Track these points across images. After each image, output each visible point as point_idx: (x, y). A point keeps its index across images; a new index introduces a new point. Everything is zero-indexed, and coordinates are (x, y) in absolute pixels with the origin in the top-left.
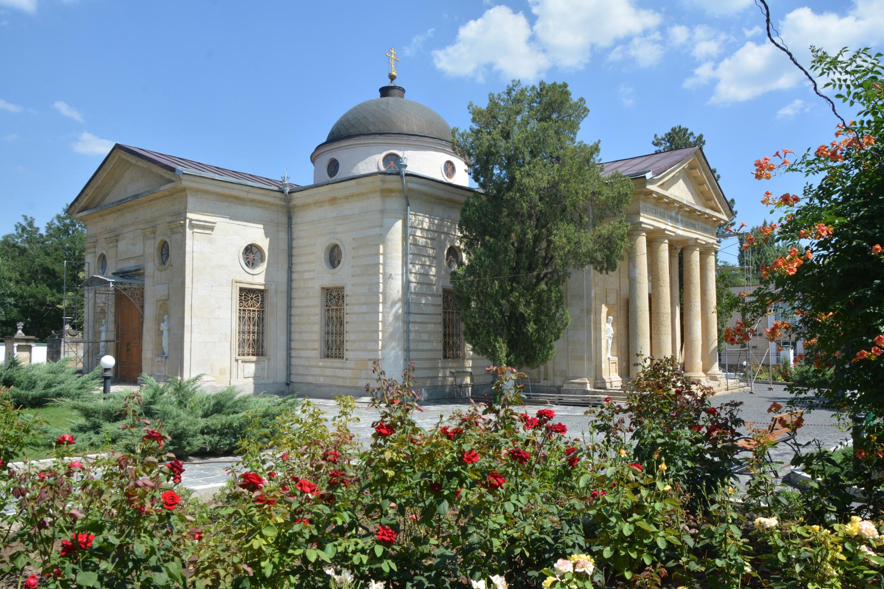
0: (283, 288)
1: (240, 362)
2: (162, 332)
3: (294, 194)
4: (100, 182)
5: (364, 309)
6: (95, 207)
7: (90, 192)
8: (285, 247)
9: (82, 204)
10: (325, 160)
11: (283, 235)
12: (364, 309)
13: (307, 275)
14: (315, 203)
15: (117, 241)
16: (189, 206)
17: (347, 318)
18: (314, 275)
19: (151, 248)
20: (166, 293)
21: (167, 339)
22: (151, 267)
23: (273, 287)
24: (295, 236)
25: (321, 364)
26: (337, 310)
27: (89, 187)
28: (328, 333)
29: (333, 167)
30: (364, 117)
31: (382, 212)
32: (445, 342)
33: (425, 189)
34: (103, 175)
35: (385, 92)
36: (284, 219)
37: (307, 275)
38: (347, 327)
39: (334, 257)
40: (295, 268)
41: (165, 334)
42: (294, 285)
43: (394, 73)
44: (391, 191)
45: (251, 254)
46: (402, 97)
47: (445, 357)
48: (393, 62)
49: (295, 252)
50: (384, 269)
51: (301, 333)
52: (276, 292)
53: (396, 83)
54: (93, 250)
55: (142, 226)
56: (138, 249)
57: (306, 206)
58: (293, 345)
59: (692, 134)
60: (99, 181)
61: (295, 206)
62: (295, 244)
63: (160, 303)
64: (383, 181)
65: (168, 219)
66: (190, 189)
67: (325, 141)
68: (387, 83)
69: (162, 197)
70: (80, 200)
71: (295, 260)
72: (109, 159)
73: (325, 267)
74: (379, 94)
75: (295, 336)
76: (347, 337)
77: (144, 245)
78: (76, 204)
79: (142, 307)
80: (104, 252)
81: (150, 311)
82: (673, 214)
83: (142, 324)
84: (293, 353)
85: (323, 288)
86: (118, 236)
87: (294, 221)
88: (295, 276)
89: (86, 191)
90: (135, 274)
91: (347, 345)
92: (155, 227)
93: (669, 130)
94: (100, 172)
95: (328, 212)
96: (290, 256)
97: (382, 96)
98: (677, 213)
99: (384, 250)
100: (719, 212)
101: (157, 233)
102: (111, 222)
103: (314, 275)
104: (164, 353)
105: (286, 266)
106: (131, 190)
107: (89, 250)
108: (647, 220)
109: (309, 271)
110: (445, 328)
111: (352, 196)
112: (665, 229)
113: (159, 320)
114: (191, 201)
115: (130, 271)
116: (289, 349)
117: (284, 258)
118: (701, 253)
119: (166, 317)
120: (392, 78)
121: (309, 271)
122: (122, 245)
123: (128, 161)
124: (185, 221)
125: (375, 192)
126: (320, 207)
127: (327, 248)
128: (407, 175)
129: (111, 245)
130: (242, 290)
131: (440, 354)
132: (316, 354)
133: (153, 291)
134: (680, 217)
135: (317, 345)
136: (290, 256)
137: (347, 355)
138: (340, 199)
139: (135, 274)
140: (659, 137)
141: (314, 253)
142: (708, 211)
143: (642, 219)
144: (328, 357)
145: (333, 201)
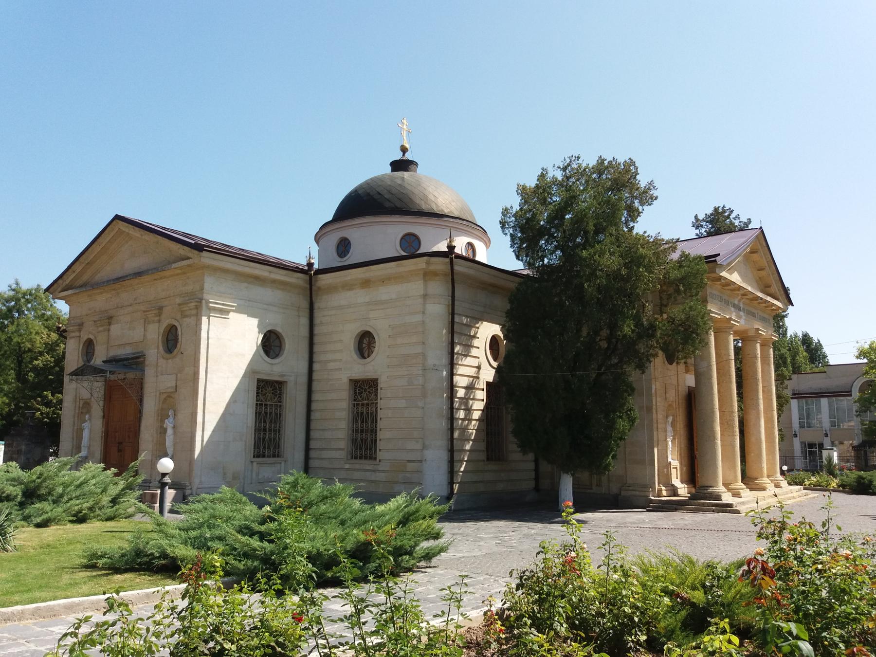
0: (304, 379)
1: (255, 464)
2: (165, 430)
5: (402, 403)
6: (81, 286)
7: (78, 268)
9: (67, 282)
10: (333, 239)
11: (305, 321)
13: (331, 366)
15: (110, 324)
16: (207, 286)
17: (380, 414)
18: (341, 365)
19: (155, 333)
21: (172, 437)
22: (154, 353)
23: (292, 378)
24: (317, 321)
25: (347, 466)
26: (368, 404)
27: (77, 263)
28: (357, 431)
29: (344, 247)
30: (379, 193)
31: (425, 296)
32: (488, 442)
33: (471, 272)
34: (97, 248)
36: (305, 304)
37: (331, 366)
38: (381, 424)
39: (365, 343)
40: (316, 358)
41: (170, 431)
42: (315, 376)
43: (407, 146)
44: (435, 274)
45: (271, 343)
46: (415, 171)
47: (488, 459)
48: (404, 134)
49: (316, 339)
51: (323, 430)
52: (296, 383)
53: (409, 156)
54: (77, 334)
55: (142, 308)
56: (137, 334)
57: (332, 289)
58: (313, 444)
59: (738, 217)
60: (90, 256)
61: (319, 288)
62: (317, 330)
64: (428, 263)
65: (178, 300)
66: (208, 267)
67: (330, 219)
68: (398, 156)
69: (172, 276)
70: (64, 277)
71: (316, 348)
72: (107, 231)
73: (355, 357)
76: (381, 435)
78: (60, 281)
79: (141, 401)
80: (91, 337)
81: (150, 406)
82: (736, 302)
83: (139, 420)
84: (312, 454)
85: (351, 380)
86: (111, 318)
87: (316, 306)
88: (316, 366)
90: (134, 362)
91: (380, 445)
92: (161, 308)
93: (710, 211)
94: (94, 246)
95: (360, 296)
96: (311, 344)
97: (393, 170)
98: (739, 301)
100: (777, 299)
101: (163, 316)
102: (101, 301)
103: (341, 365)
105: (306, 356)
106: (132, 265)
107: (72, 334)
108: (715, 310)
109: (335, 361)
110: (487, 425)
112: (730, 319)
113: (162, 416)
114: (209, 282)
115: (127, 359)
116: (307, 449)
118: (761, 346)
119: (171, 413)
120: (404, 150)
121: (335, 361)
122: (115, 329)
123: (128, 234)
127: (358, 335)
129: (101, 329)
130: (259, 380)
131: (483, 456)
132: (342, 454)
133: (156, 381)
134: (741, 305)
135: (342, 444)
136: (311, 344)
137: (380, 455)
139: (134, 362)
140: (701, 217)
141: (341, 341)
142: (769, 299)
143: (710, 307)
144: (356, 458)
145: (366, 283)
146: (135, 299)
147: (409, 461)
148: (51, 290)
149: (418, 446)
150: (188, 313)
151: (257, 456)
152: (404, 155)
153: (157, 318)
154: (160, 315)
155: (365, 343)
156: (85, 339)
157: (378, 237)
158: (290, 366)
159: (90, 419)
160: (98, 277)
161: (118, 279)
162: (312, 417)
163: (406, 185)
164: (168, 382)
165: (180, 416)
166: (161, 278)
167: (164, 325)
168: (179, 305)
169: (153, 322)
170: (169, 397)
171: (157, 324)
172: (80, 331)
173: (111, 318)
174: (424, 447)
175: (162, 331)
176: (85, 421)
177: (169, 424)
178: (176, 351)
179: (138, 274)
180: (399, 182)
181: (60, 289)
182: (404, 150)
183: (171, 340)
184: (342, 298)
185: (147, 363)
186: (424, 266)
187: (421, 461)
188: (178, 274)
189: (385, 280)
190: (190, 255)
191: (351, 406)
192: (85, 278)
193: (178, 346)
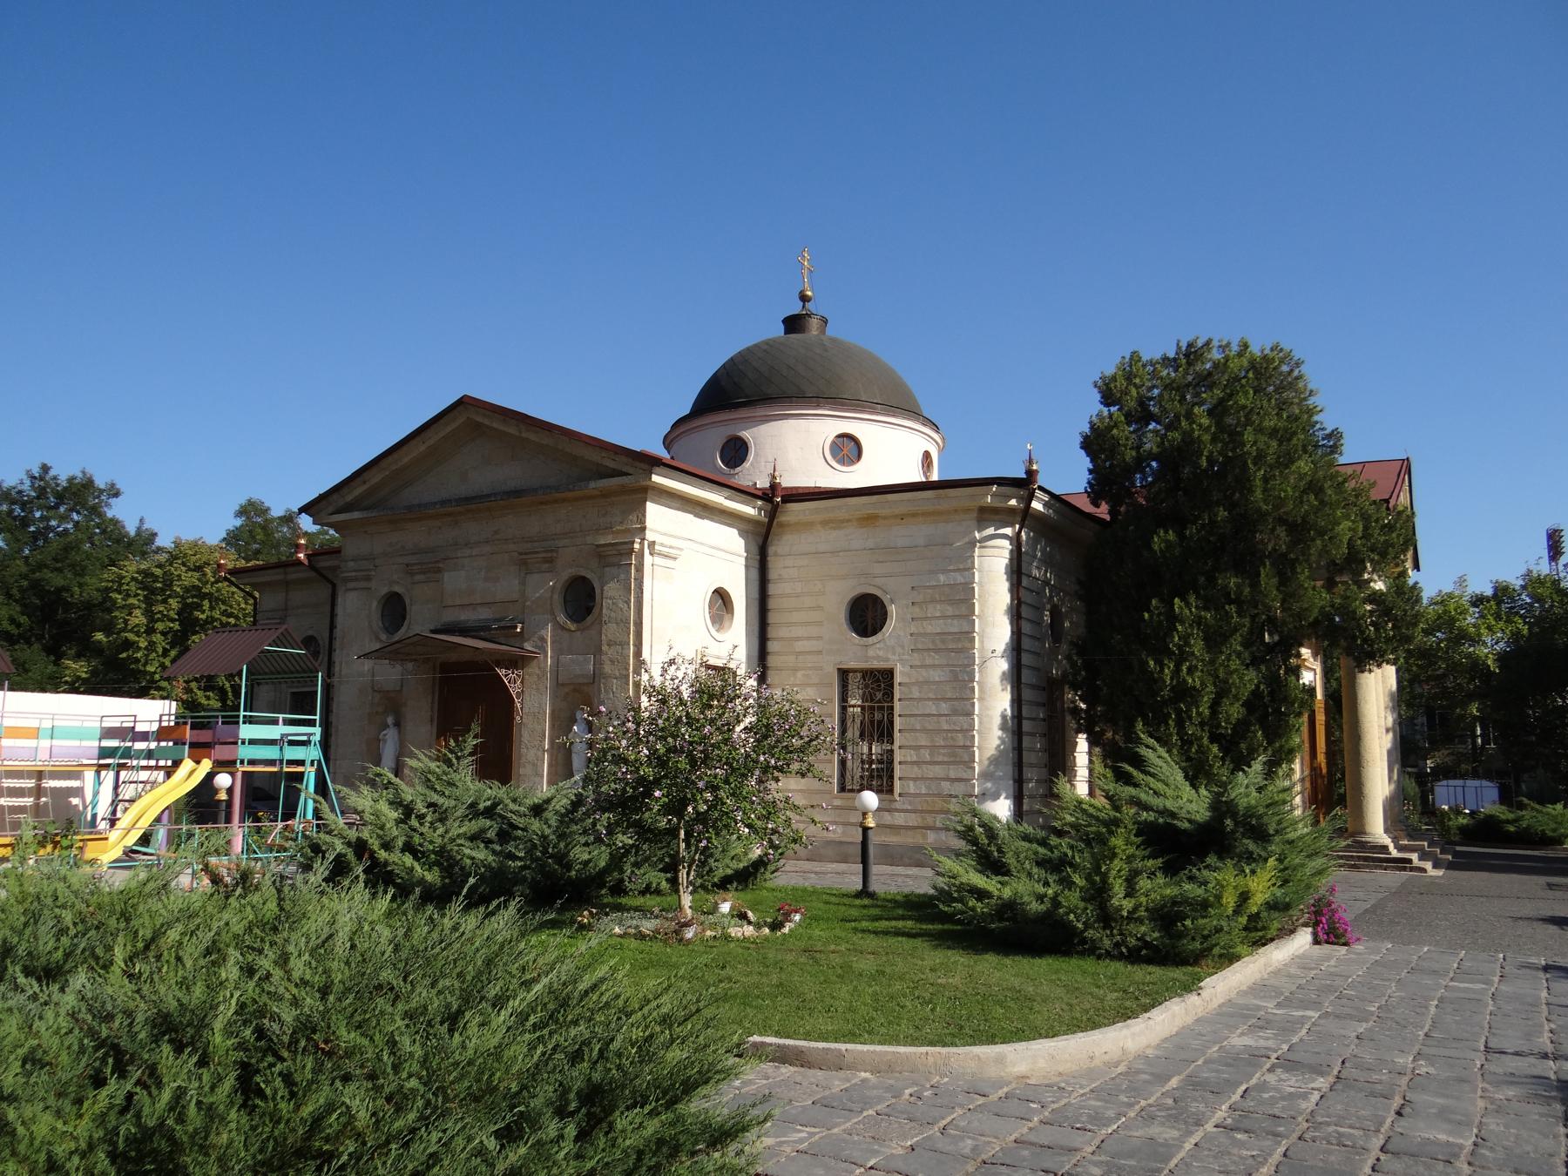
4: (406, 460)
7: (375, 478)
9: (349, 498)
12: (944, 707)
14: (825, 523)
19: (546, 586)
35: (794, 324)
39: (866, 615)
48: (805, 272)
50: (982, 642)
57: (807, 526)
60: (405, 458)
62: (772, 589)
68: (796, 308)
71: (772, 618)
74: (782, 327)
77: (523, 583)
78: (335, 496)
80: (397, 589)
89: (366, 475)
94: (414, 442)
99: (982, 611)
107: (351, 585)
111: (914, 515)
113: (563, 723)
117: (755, 609)
120: (804, 298)
122: (454, 580)
124: (642, 544)
125: (968, 510)
129: (418, 577)
138: (885, 518)
145: (869, 520)
146: (496, 532)
154: (550, 561)
155: (866, 615)
156: (384, 590)
159: (397, 724)
166: (556, 501)
176: (386, 726)
181: (331, 509)
182: (804, 298)
190: (630, 471)
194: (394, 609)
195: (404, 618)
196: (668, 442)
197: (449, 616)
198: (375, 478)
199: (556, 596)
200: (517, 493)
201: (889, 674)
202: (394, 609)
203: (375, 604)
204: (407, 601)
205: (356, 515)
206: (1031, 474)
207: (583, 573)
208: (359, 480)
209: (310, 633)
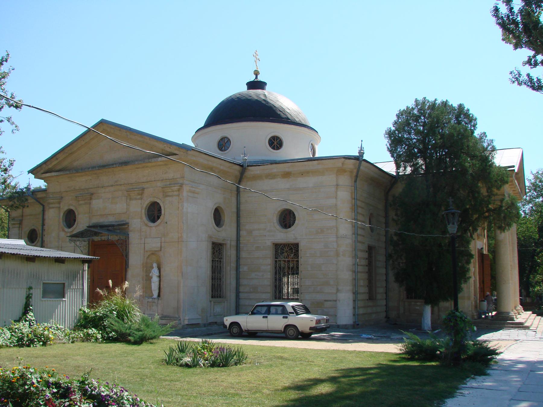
0: (234, 243)
1: (212, 302)
3: (250, 168)
7: (61, 156)
8: (235, 210)
9: (50, 166)
15: (91, 199)
18: (266, 233)
20: (159, 245)
22: (138, 222)
23: (229, 242)
53: (260, 78)
54: (57, 205)
57: (256, 178)
58: (241, 289)
62: (242, 207)
63: (149, 253)
65: (159, 184)
68: (252, 78)
70: (49, 163)
71: (242, 221)
73: (278, 227)
74: (246, 87)
75: (243, 282)
84: (242, 295)
86: (92, 194)
88: (243, 233)
92: (143, 189)
102: (82, 182)
104: (151, 296)
105: (235, 225)
107: (51, 206)
113: (147, 269)
115: (113, 226)
116: (238, 293)
122: (97, 204)
126: (271, 179)
128: (365, 160)
129: (81, 202)
139: (120, 228)
145: (287, 175)
146: (116, 182)
147: (326, 301)
148: (35, 172)
149: (334, 291)
150: (170, 194)
151: (212, 297)
152: (256, 78)
153: (139, 197)
154: (142, 194)
155: (287, 219)
156: (66, 208)
157: (249, 137)
158: (226, 234)
160: (76, 164)
161: (104, 166)
162: (241, 270)
163: (269, 100)
164: (153, 244)
165: (166, 269)
166: (143, 167)
167: (146, 202)
168: (163, 188)
169: (136, 199)
170: (153, 254)
171: (140, 201)
172: (59, 203)
173: (92, 194)
174: (338, 290)
175: (145, 206)
177: (155, 272)
178: (159, 221)
179: (125, 163)
180: (263, 98)
181: (42, 171)
182: (256, 73)
183: (154, 213)
184: (266, 184)
185: (131, 228)
186: (340, 165)
187: (336, 301)
188: (159, 165)
189: (303, 174)
191: (274, 262)
192: (65, 164)
193: (162, 217)
194: (70, 218)
195: (75, 221)
196: (194, 139)
197: (95, 221)
198: (61, 156)
199: (143, 211)
200: (125, 163)
201: (296, 246)
202: (70, 218)
203: (62, 214)
204: (77, 213)
205: (53, 174)
206: (361, 153)
207: (156, 200)
208: (55, 158)
209: (33, 227)
